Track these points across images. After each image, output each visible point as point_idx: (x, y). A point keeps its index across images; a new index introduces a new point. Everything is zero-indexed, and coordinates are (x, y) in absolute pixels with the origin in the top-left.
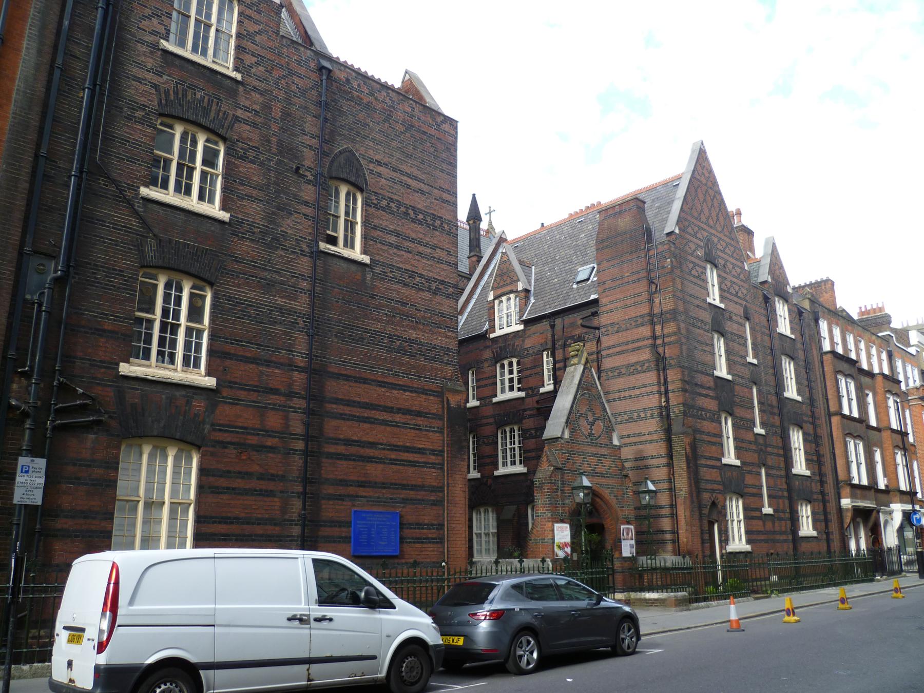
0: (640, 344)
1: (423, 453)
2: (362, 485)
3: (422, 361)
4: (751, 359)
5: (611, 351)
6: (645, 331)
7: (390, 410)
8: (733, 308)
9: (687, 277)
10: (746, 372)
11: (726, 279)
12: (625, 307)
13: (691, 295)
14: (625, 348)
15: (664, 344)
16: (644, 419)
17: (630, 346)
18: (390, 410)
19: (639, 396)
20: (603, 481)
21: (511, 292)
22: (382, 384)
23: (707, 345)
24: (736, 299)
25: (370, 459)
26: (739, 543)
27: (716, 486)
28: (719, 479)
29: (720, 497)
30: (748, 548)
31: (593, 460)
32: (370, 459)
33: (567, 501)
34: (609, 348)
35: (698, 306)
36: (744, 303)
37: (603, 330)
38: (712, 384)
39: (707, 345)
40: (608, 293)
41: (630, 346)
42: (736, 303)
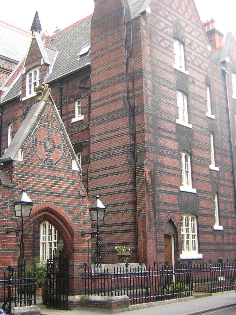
0: (117, 97)
4: (209, 114)
5: (97, 104)
6: (122, 87)
8: (195, 75)
9: (156, 46)
10: (205, 124)
11: (191, 53)
12: (108, 69)
13: (158, 61)
14: (106, 101)
15: (134, 97)
16: (117, 155)
17: (110, 99)
19: (114, 137)
20: (59, 200)
21: (37, 66)
23: (171, 99)
24: (199, 69)
26: (190, 253)
27: (173, 208)
28: (177, 202)
29: (177, 216)
30: (200, 256)
31: (50, 182)
34: (96, 102)
35: (164, 70)
36: (206, 73)
37: (92, 89)
38: (174, 129)
39: (171, 99)
40: (97, 60)
41: (110, 99)
42: (199, 72)
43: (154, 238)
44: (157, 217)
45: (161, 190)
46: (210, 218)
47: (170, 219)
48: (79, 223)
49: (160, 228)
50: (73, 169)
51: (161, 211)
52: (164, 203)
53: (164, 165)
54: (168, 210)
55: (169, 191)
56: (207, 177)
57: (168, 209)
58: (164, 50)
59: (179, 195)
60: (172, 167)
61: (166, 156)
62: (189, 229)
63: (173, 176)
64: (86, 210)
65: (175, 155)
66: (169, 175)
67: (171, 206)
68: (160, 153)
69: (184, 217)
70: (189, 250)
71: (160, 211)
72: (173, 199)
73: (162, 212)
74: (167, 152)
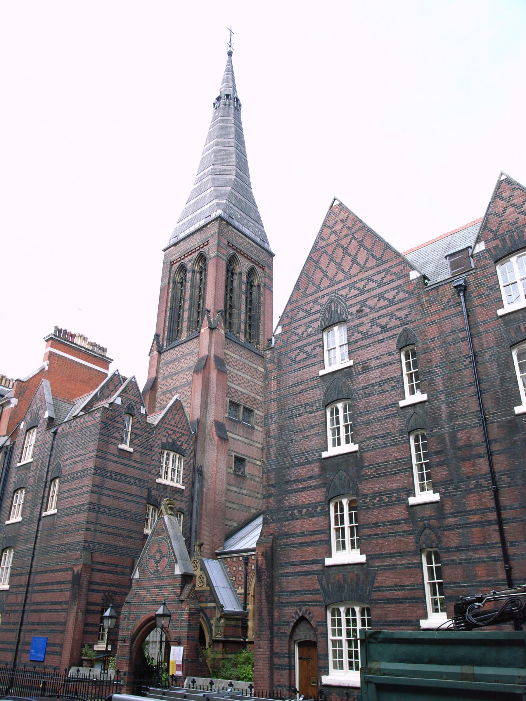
1: (61, 604)
2: (38, 624)
3: (69, 553)
7: (52, 584)
18: (52, 584)
22: (52, 571)
25: (42, 611)
28: (317, 586)
29: (316, 611)
31: (154, 592)
32: (42, 611)
33: (130, 627)
43: (266, 647)
44: (276, 614)
45: (287, 573)
46: (407, 605)
47: (301, 615)
48: (177, 629)
50: (176, 573)
51: (283, 605)
52: (291, 592)
53: (294, 534)
54: (298, 602)
55: (302, 572)
56: (401, 523)
57: (297, 600)
59: (323, 573)
60: (309, 531)
61: (298, 519)
63: (310, 546)
64: (184, 615)
65: (315, 511)
66: (301, 546)
67: (305, 594)
68: (288, 517)
69: (342, 609)
71: (282, 606)
72: (311, 582)
73: (285, 606)
74: (300, 512)
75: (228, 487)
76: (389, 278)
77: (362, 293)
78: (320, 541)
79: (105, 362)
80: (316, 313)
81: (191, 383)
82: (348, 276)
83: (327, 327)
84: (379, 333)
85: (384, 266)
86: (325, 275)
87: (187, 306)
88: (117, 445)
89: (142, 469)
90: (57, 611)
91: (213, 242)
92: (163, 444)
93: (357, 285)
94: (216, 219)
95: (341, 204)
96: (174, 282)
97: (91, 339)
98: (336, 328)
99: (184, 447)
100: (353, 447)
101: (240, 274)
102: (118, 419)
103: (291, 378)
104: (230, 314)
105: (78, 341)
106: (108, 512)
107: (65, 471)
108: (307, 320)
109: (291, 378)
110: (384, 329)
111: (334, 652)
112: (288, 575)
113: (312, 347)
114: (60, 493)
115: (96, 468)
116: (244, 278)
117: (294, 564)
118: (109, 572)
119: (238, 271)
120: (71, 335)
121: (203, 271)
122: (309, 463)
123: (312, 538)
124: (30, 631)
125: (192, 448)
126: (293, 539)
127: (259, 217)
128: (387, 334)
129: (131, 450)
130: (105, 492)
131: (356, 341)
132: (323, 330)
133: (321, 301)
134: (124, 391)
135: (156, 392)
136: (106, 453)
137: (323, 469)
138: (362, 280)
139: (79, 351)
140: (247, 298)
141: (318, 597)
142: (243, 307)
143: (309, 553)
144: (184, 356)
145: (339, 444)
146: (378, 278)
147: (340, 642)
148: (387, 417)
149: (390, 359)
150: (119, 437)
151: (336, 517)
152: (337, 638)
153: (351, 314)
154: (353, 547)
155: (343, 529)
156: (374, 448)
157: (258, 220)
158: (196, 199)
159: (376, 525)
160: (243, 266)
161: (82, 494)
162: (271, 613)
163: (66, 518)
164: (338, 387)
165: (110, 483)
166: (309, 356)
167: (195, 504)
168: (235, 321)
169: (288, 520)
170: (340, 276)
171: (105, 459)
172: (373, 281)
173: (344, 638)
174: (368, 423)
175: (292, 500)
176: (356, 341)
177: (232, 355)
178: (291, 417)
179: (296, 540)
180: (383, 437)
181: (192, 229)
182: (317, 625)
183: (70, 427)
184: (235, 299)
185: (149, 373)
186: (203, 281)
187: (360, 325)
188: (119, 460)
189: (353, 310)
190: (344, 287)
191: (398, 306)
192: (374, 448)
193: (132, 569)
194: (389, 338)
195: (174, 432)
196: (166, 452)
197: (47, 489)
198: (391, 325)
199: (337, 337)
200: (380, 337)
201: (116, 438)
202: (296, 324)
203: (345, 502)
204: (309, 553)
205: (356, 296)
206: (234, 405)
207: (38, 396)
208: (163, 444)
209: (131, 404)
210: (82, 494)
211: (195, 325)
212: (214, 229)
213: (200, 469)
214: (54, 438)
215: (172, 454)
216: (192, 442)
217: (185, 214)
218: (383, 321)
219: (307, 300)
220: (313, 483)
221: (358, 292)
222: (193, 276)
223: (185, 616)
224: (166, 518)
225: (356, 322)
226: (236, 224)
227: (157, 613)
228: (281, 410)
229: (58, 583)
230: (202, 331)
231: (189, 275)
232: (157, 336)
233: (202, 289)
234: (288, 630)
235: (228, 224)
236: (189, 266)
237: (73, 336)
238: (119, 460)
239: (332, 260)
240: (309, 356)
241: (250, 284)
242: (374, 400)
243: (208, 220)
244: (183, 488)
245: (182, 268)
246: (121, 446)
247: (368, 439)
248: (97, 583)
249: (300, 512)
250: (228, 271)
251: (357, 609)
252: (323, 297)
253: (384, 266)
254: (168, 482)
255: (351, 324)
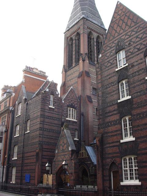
22: (31, 152)
25: (28, 166)
28: (118, 151)
29: (118, 160)
31: (62, 157)
44: (104, 162)
49: (106, 168)
57: (111, 156)
58: (112, 66)
62: (129, 165)
69: (127, 159)
70: (127, 179)
72: (116, 149)
75: (94, 120)
76: (140, 29)
77: (130, 37)
78: (118, 134)
79: (45, 77)
80: (113, 47)
81: (77, 82)
82: (124, 31)
83: (118, 52)
84: (137, 52)
85: (138, 25)
86: (116, 32)
87: (74, 53)
88: (48, 106)
89: (58, 114)
90: (32, 165)
91: (82, 27)
92: (67, 105)
93: (128, 34)
94: (82, 19)
95: (120, 3)
96: (69, 45)
97: (39, 69)
98: (121, 52)
99: (76, 106)
100: (129, 97)
101: (93, 38)
102: (48, 97)
103: (106, 74)
104: (91, 54)
105: (35, 70)
106: (47, 130)
107: (31, 117)
108: (110, 50)
109: (106, 74)
110: (139, 50)
111: (125, 174)
112: (108, 147)
113: (112, 60)
114: (30, 125)
115: (41, 115)
116: (95, 40)
117: (110, 143)
118: (49, 152)
119: (92, 37)
120: (32, 69)
121: (79, 39)
122: (113, 105)
123: (116, 133)
124: (25, 173)
125: (79, 106)
126: (109, 134)
127: (100, 16)
128: (140, 52)
129: (54, 108)
130: (45, 123)
131: (129, 56)
132: (116, 53)
133: (115, 42)
134: (49, 86)
135: (65, 86)
136: (44, 109)
137: (119, 107)
138: (130, 31)
139: (35, 74)
140: (97, 48)
141: (118, 155)
142: (95, 51)
143: (115, 139)
144: (74, 72)
145: (124, 97)
146: (135, 30)
147: (127, 170)
148: (141, 84)
149: (141, 61)
150: (49, 103)
151: (124, 124)
152: (126, 169)
153: (126, 45)
154: (131, 135)
155: (127, 128)
156: (137, 97)
157: (99, 17)
158: (74, 12)
159: (138, 126)
160: (95, 35)
161: (37, 124)
162: (102, 161)
163: (33, 134)
164: (123, 74)
165: (47, 120)
166: (112, 64)
167: (82, 127)
168: (93, 57)
169: (107, 127)
170: (122, 31)
171: (44, 111)
172: (134, 31)
173: (128, 169)
174: (134, 87)
175: (108, 120)
176: (129, 56)
177: (93, 70)
178: (106, 89)
179: (110, 134)
180: (140, 92)
181: (74, 24)
182: (118, 165)
183: (32, 101)
184: (92, 48)
185: (62, 80)
186: (79, 43)
187: (130, 49)
188: (49, 111)
189: (127, 44)
190: (123, 36)
191: (143, 40)
192: (137, 97)
193: (55, 150)
194: (141, 53)
195: (72, 101)
196: (69, 108)
197: (26, 124)
198: (141, 48)
199: (122, 55)
200: (137, 53)
201: (48, 104)
202: (107, 52)
203: (127, 118)
204: (115, 139)
205: (128, 38)
206: (94, 88)
207: (21, 92)
208: (67, 105)
209: (52, 91)
210: (37, 124)
211: (77, 60)
212: (82, 22)
213: (83, 114)
214: (27, 105)
215: (71, 109)
216: (79, 104)
217: (71, 18)
218: (138, 47)
219: (110, 42)
220: (115, 112)
221: (128, 37)
222: (75, 41)
223: (73, 165)
224: (65, 130)
225: (128, 48)
226: (90, 19)
227: (63, 164)
228: (103, 86)
229: (32, 156)
230: (80, 62)
231: (74, 41)
232: (64, 66)
233: (78, 46)
234: (108, 167)
235: (87, 20)
236: (74, 38)
237: (33, 69)
238: (49, 111)
239: (118, 26)
240: (112, 64)
241: (98, 42)
242: (136, 78)
243: (79, 19)
244: (77, 121)
245: (71, 39)
246: (49, 107)
247: (135, 93)
248: (45, 156)
249: (111, 124)
250: (88, 38)
251: (133, 158)
252: (116, 40)
253: (138, 25)
254: (71, 119)
255: (127, 49)
